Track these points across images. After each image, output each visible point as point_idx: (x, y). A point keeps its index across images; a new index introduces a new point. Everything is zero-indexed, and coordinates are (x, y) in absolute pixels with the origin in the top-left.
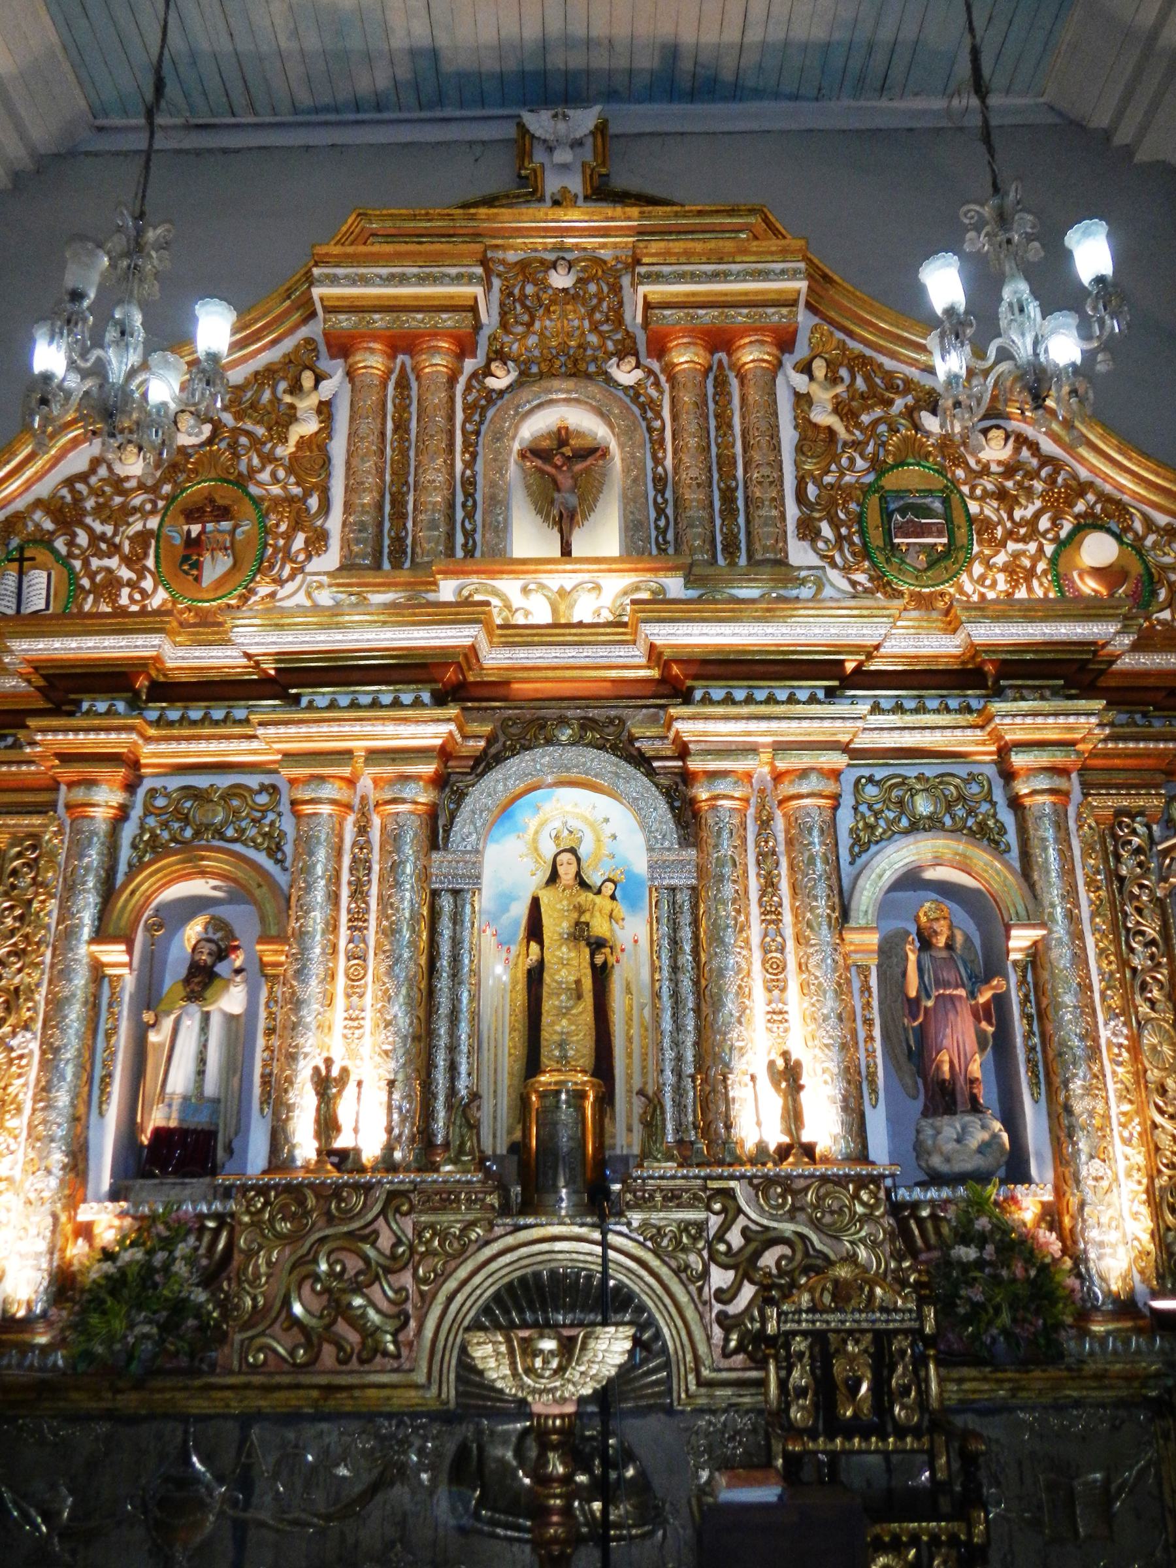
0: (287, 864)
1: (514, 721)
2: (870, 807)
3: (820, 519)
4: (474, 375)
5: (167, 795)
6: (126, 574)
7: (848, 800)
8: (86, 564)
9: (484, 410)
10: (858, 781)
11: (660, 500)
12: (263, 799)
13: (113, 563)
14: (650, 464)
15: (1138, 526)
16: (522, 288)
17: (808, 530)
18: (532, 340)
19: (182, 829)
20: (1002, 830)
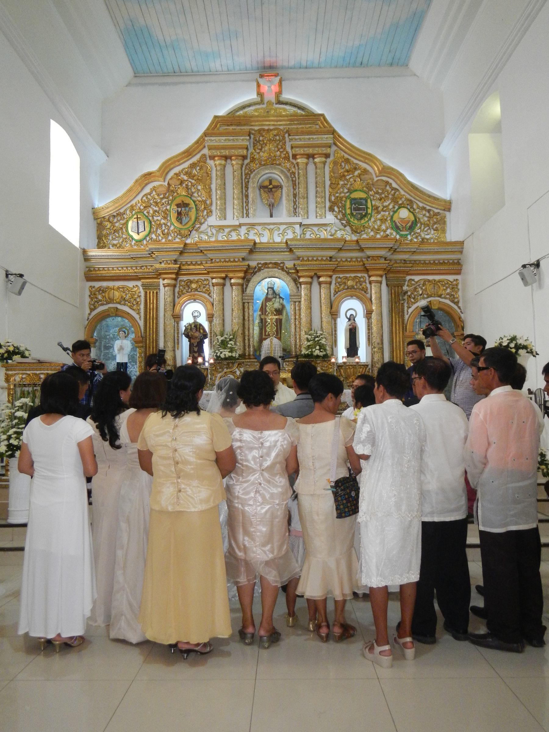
0: (212, 297)
1: (260, 263)
2: (339, 283)
3: (334, 206)
4: (247, 164)
5: (185, 282)
6: (163, 221)
7: (334, 282)
8: (153, 218)
9: (250, 175)
10: (337, 277)
11: (295, 200)
12: (205, 282)
13: (159, 218)
14: (292, 190)
15: (415, 207)
16: (259, 138)
17: (331, 209)
18: (261, 154)
19: (188, 289)
20: (367, 288)
